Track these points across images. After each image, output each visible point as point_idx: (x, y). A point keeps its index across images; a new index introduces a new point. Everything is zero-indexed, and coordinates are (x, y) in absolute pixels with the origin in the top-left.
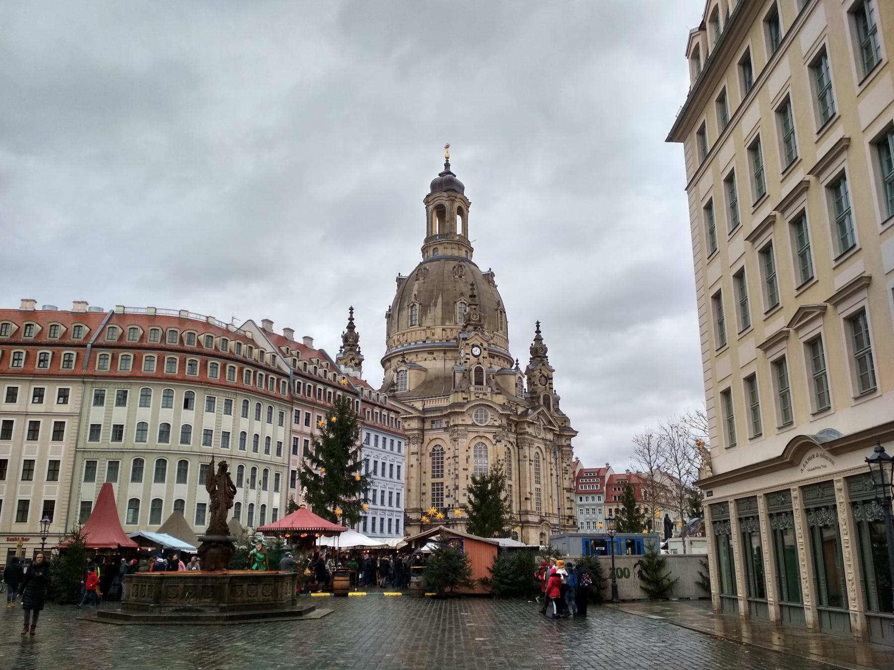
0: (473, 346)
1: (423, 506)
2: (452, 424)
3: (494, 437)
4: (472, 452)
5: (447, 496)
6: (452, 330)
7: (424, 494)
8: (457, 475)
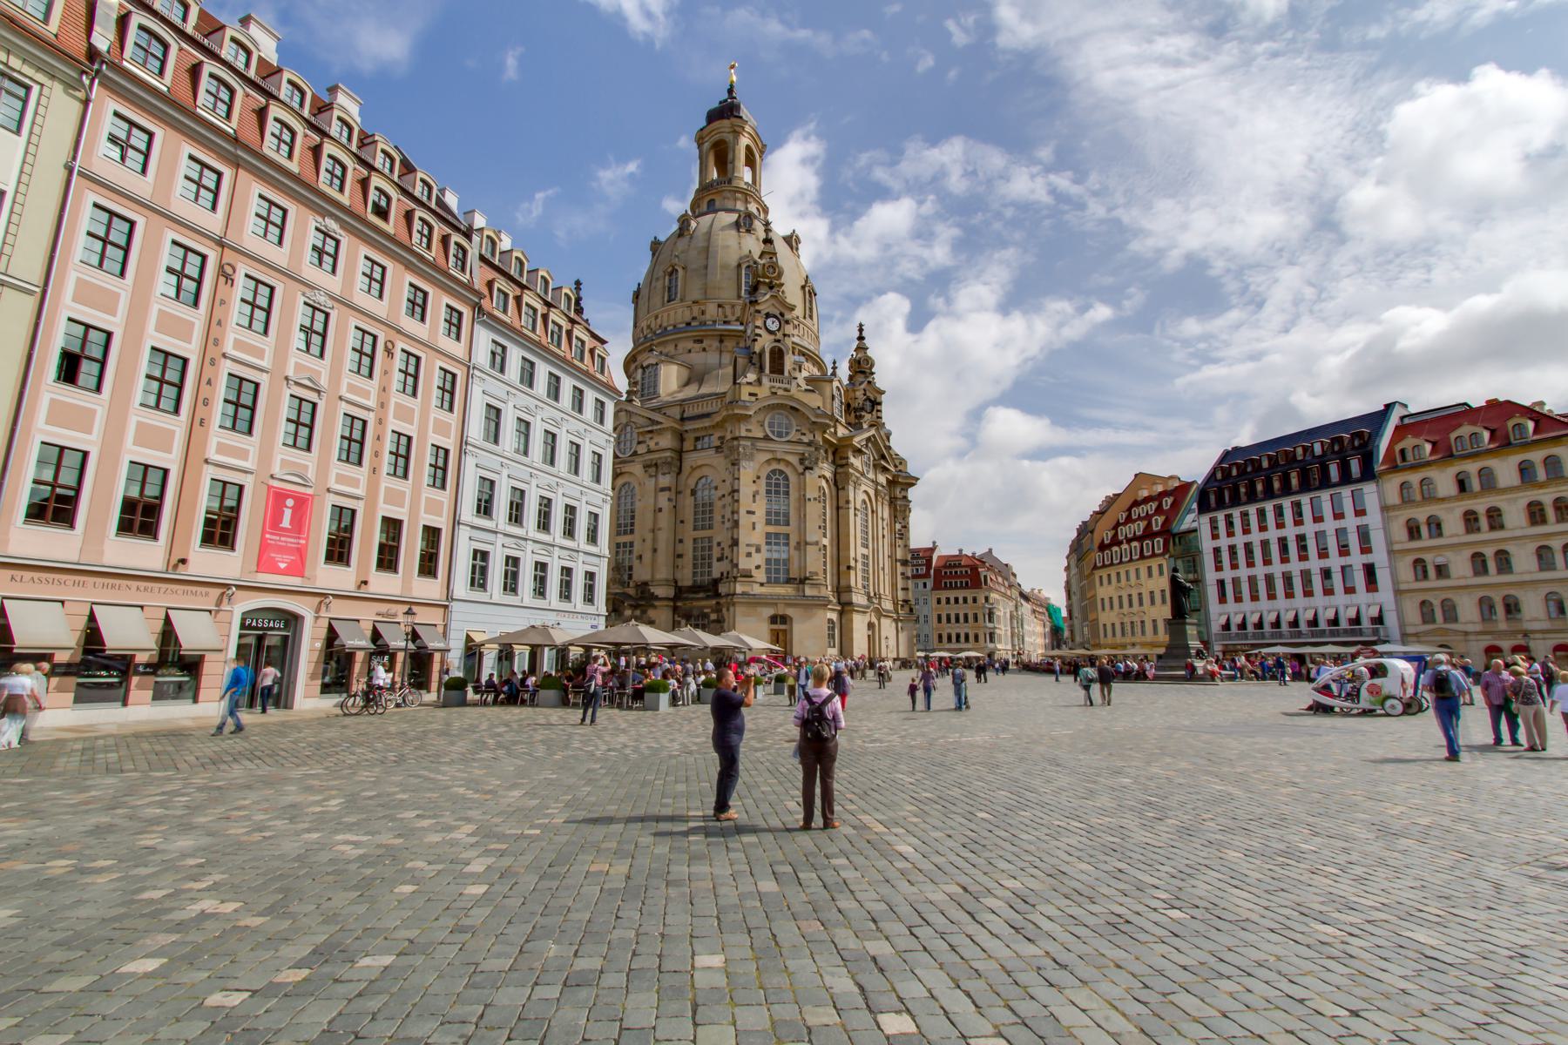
0: (768, 316)
1: (679, 576)
2: (729, 436)
3: (802, 461)
4: (762, 486)
5: (719, 560)
6: (733, 306)
7: (680, 556)
8: (736, 524)
